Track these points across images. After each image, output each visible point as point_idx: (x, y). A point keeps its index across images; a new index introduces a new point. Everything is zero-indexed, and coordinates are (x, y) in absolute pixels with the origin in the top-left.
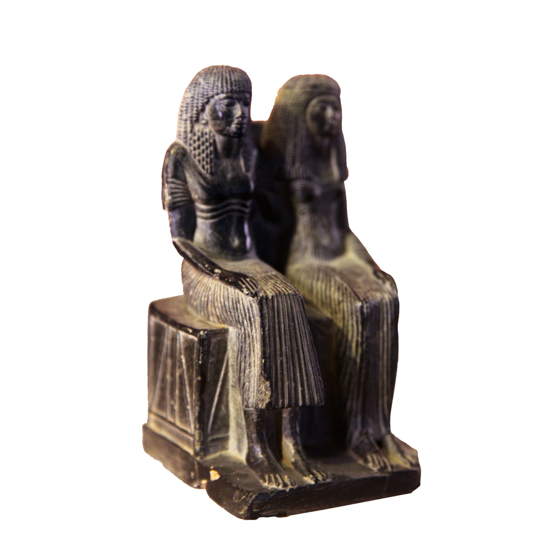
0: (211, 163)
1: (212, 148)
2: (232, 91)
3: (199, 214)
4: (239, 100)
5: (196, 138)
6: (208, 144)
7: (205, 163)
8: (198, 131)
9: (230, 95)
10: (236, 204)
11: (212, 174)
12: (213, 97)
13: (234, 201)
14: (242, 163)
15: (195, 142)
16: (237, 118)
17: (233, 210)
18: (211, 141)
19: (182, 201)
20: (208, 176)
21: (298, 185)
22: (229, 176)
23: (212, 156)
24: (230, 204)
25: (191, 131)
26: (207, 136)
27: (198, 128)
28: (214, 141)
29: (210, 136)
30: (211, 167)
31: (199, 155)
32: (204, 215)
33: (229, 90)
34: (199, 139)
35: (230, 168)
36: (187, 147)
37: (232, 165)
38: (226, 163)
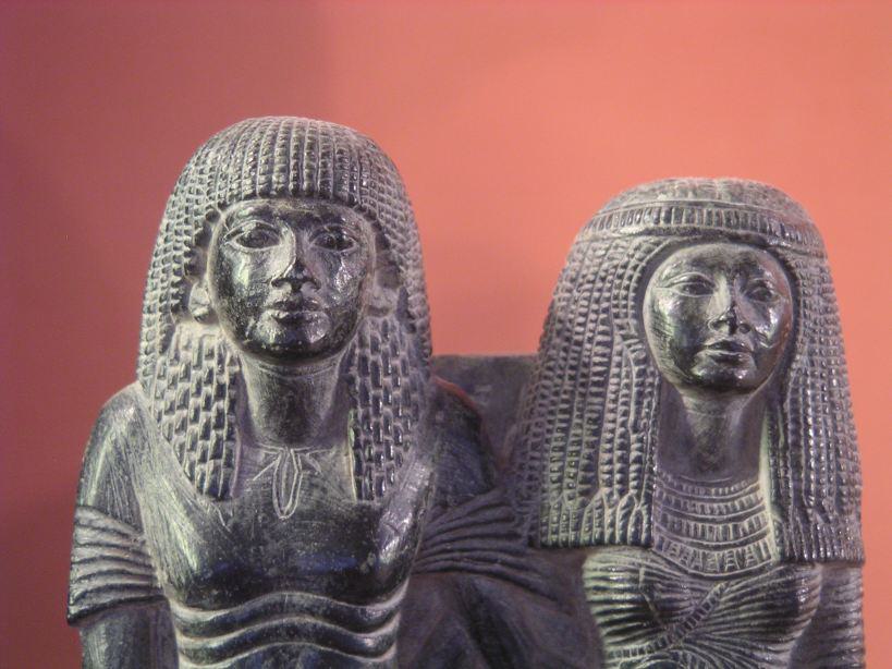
0: (216, 456)
1: (224, 404)
2: (265, 194)
3: (182, 640)
4: (300, 223)
5: (180, 369)
6: (210, 390)
7: (196, 456)
8: (186, 348)
9: (260, 202)
10: (310, 611)
11: (218, 493)
12: (212, 217)
13: (299, 597)
14: (347, 463)
15: (174, 383)
16: (278, 283)
17: (294, 632)
18: (226, 379)
19: (111, 588)
20: (203, 501)
21: (610, 574)
22: (288, 508)
23: (224, 433)
24: (279, 609)
25: (165, 347)
26: (213, 363)
27: (189, 332)
28: (237, 380)
29: (221, 361)
30: (216, 470)
31: (183, 427)
32: (197, 643)
33: (259, 188)
34: (187, 375)
35: (299, 477)
36: (147, 402)
37: (306, 466)
38: (276, 459)
